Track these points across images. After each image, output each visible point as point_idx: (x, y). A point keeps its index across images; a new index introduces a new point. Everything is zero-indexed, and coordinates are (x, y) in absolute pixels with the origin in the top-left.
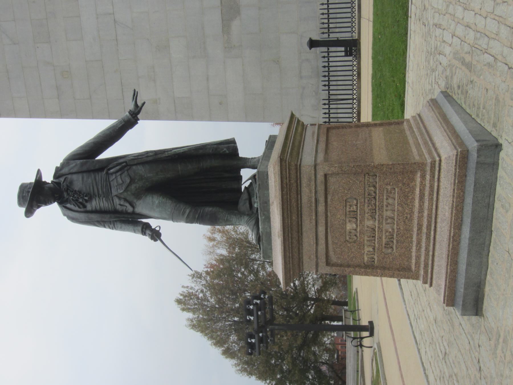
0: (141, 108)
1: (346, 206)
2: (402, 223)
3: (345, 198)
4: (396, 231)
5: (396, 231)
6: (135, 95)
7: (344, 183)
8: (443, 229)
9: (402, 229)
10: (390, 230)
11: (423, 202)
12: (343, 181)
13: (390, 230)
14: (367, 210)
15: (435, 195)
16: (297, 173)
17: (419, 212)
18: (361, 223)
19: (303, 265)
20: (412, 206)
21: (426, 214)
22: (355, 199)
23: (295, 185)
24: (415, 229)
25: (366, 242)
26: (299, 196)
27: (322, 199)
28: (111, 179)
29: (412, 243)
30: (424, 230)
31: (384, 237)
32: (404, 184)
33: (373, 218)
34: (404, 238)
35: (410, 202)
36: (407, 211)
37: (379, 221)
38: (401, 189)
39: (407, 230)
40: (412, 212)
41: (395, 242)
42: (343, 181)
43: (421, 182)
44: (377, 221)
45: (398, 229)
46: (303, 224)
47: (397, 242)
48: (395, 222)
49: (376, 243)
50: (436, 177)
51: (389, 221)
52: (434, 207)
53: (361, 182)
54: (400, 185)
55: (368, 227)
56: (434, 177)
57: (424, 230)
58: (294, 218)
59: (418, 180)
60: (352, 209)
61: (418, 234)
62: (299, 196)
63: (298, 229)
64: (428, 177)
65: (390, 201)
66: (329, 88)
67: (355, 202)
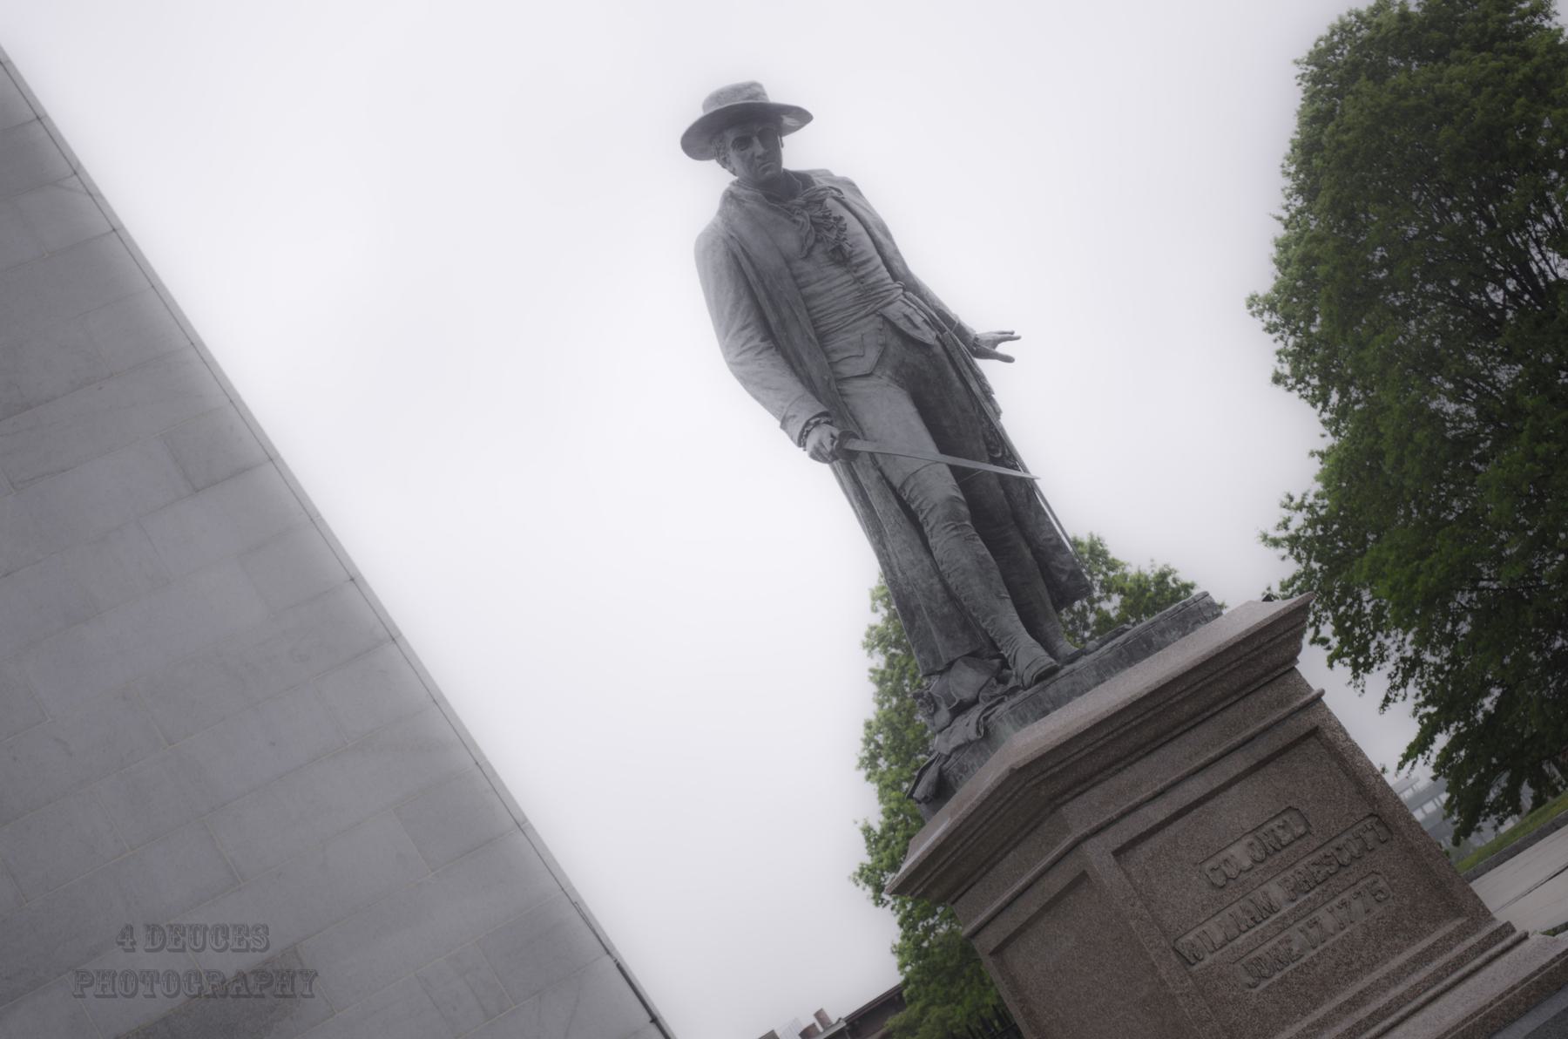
1: (1277, 816)
3: (1293, 803)
4: (1303, 960)
5: (1303, 960)
6: (1009, 337)
10: (1295, 949)
11: (1414, 970)
13: (1295, 949)
14: (1300, 867)
15: (1455, 977)
17: (1387, 977)
19: (1114, 774)
21: (1394, 992)
22: (1308, 825)
24: (1341, 999)
25: (1226, 913)
26: (1235, 698)
27: (1262, 749)
29: (1304, 1015)
30: (1362, 1013)
31: (1269, 945)
33: (1296, 890)
37: (1298, 908)
38: (1398, 909)
40: (1370, 966)
41: (1277, 976)
43: (1450, 936)
44: (1294, 905)
45: (1312, 964)
46: (1176, 742)
47: (1283, 980)
48: (1320, 948)
49: (1243, 937)
51: (1314, 932)
52: (1431, 993)
53: (1352, 814)
54: (1407, 902)
55: (1265, 894)
56: (1483, 951)
57: (1362, 1013)
58: (1187, 707)
59: (1449, 927)
60: (1280, 833)
61: (1339, 1009)
62: (1235, 698)
64: (1472, 941)
65: (1357, 905)
67: (1301, 830)
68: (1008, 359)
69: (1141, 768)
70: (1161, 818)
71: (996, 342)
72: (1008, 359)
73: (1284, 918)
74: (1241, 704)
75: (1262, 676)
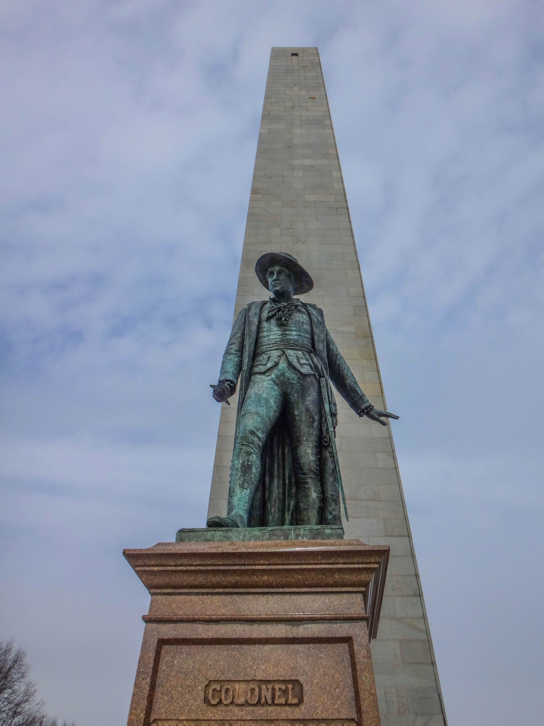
16: (353, 585)
62: (306, 590)
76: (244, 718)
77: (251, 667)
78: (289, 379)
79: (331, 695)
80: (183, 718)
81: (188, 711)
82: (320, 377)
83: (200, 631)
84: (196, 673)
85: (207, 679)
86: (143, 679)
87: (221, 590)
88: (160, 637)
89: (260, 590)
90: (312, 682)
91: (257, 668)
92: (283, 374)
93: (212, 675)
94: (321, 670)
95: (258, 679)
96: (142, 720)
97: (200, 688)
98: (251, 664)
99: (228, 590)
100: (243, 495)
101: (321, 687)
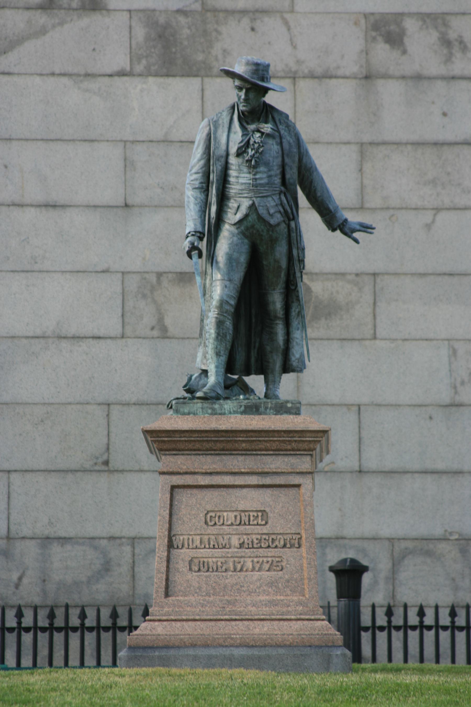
0: (350, 237)
2: (235, 582)
7: (288, 509)
8: (235, 627)
9: (227, 581)
12: (290, 508)
16: (305, 450)
18: (234, 530)
20: (259, 592)
23: (289, 447)
26: (272, 452)
27: (268, 481)
28: (274, 197)
32: (288, 581)
33: (241, 545)
34: (214, 585)
35: (264, 590)
36: (251, 586)
38: (281, 578)
39: (224, 587)
42: (290, 508)
46: (232, 457)
50: (303, 617)
54: (287, 577)
56: (301, 614)
62: (272, 452)
63: (227, 450)
66: (43, 630)
68: (356, 241)
69: (209, 459)
70: (202, 483)
71: (354, 231)
72: (356, 241)
73: (228, 553)
74: (274, 457)
75: (290, 450)
76: (231, 533)
77: (235, 503)
78: (258, 231)
79: (286, 519)
80: (192, 533)
81: (195, 529)
82: (289, 220)
83: (199, 480)
84: (198, 506)
85: (206, 510)
86: (164, 511)
87: (213, 452)
88: (172, 484)
89: (240, 452)
90: (274, 512)
91: (239, 503)
92: (253, 226)
93: (209, 507)
94: (281, 504)
95: (239, 509)
96: (167, 536)
97: (201, 515)
98: (235, 500)
99: (217, 452)
100: (220, 362)
101: (280, 515)
